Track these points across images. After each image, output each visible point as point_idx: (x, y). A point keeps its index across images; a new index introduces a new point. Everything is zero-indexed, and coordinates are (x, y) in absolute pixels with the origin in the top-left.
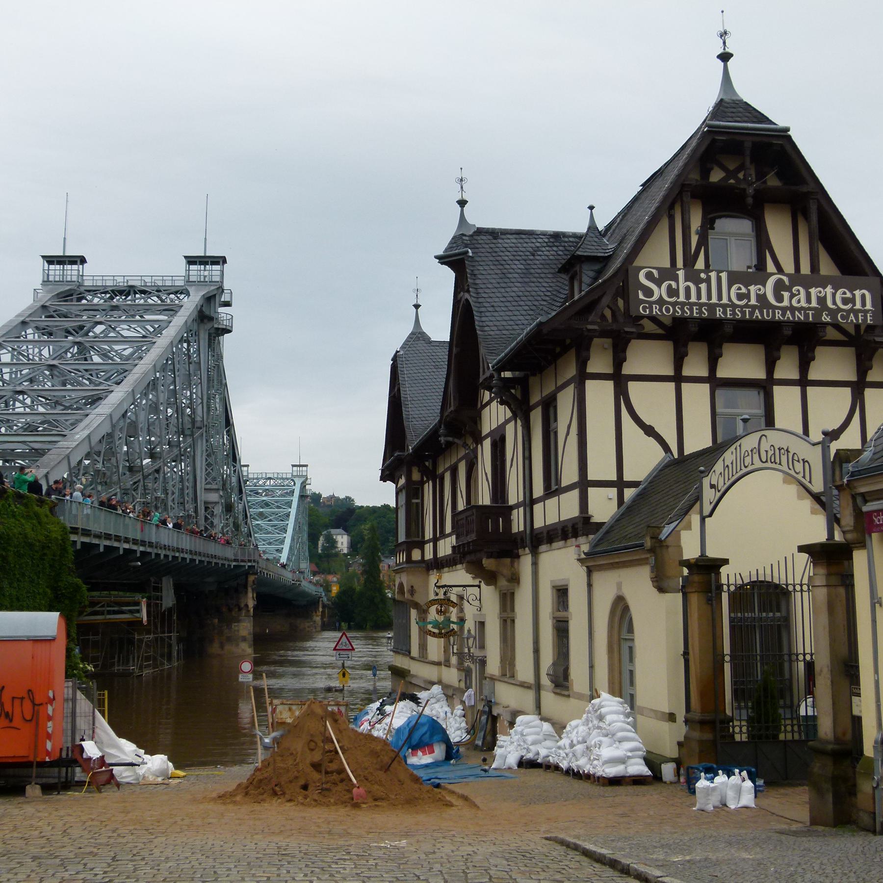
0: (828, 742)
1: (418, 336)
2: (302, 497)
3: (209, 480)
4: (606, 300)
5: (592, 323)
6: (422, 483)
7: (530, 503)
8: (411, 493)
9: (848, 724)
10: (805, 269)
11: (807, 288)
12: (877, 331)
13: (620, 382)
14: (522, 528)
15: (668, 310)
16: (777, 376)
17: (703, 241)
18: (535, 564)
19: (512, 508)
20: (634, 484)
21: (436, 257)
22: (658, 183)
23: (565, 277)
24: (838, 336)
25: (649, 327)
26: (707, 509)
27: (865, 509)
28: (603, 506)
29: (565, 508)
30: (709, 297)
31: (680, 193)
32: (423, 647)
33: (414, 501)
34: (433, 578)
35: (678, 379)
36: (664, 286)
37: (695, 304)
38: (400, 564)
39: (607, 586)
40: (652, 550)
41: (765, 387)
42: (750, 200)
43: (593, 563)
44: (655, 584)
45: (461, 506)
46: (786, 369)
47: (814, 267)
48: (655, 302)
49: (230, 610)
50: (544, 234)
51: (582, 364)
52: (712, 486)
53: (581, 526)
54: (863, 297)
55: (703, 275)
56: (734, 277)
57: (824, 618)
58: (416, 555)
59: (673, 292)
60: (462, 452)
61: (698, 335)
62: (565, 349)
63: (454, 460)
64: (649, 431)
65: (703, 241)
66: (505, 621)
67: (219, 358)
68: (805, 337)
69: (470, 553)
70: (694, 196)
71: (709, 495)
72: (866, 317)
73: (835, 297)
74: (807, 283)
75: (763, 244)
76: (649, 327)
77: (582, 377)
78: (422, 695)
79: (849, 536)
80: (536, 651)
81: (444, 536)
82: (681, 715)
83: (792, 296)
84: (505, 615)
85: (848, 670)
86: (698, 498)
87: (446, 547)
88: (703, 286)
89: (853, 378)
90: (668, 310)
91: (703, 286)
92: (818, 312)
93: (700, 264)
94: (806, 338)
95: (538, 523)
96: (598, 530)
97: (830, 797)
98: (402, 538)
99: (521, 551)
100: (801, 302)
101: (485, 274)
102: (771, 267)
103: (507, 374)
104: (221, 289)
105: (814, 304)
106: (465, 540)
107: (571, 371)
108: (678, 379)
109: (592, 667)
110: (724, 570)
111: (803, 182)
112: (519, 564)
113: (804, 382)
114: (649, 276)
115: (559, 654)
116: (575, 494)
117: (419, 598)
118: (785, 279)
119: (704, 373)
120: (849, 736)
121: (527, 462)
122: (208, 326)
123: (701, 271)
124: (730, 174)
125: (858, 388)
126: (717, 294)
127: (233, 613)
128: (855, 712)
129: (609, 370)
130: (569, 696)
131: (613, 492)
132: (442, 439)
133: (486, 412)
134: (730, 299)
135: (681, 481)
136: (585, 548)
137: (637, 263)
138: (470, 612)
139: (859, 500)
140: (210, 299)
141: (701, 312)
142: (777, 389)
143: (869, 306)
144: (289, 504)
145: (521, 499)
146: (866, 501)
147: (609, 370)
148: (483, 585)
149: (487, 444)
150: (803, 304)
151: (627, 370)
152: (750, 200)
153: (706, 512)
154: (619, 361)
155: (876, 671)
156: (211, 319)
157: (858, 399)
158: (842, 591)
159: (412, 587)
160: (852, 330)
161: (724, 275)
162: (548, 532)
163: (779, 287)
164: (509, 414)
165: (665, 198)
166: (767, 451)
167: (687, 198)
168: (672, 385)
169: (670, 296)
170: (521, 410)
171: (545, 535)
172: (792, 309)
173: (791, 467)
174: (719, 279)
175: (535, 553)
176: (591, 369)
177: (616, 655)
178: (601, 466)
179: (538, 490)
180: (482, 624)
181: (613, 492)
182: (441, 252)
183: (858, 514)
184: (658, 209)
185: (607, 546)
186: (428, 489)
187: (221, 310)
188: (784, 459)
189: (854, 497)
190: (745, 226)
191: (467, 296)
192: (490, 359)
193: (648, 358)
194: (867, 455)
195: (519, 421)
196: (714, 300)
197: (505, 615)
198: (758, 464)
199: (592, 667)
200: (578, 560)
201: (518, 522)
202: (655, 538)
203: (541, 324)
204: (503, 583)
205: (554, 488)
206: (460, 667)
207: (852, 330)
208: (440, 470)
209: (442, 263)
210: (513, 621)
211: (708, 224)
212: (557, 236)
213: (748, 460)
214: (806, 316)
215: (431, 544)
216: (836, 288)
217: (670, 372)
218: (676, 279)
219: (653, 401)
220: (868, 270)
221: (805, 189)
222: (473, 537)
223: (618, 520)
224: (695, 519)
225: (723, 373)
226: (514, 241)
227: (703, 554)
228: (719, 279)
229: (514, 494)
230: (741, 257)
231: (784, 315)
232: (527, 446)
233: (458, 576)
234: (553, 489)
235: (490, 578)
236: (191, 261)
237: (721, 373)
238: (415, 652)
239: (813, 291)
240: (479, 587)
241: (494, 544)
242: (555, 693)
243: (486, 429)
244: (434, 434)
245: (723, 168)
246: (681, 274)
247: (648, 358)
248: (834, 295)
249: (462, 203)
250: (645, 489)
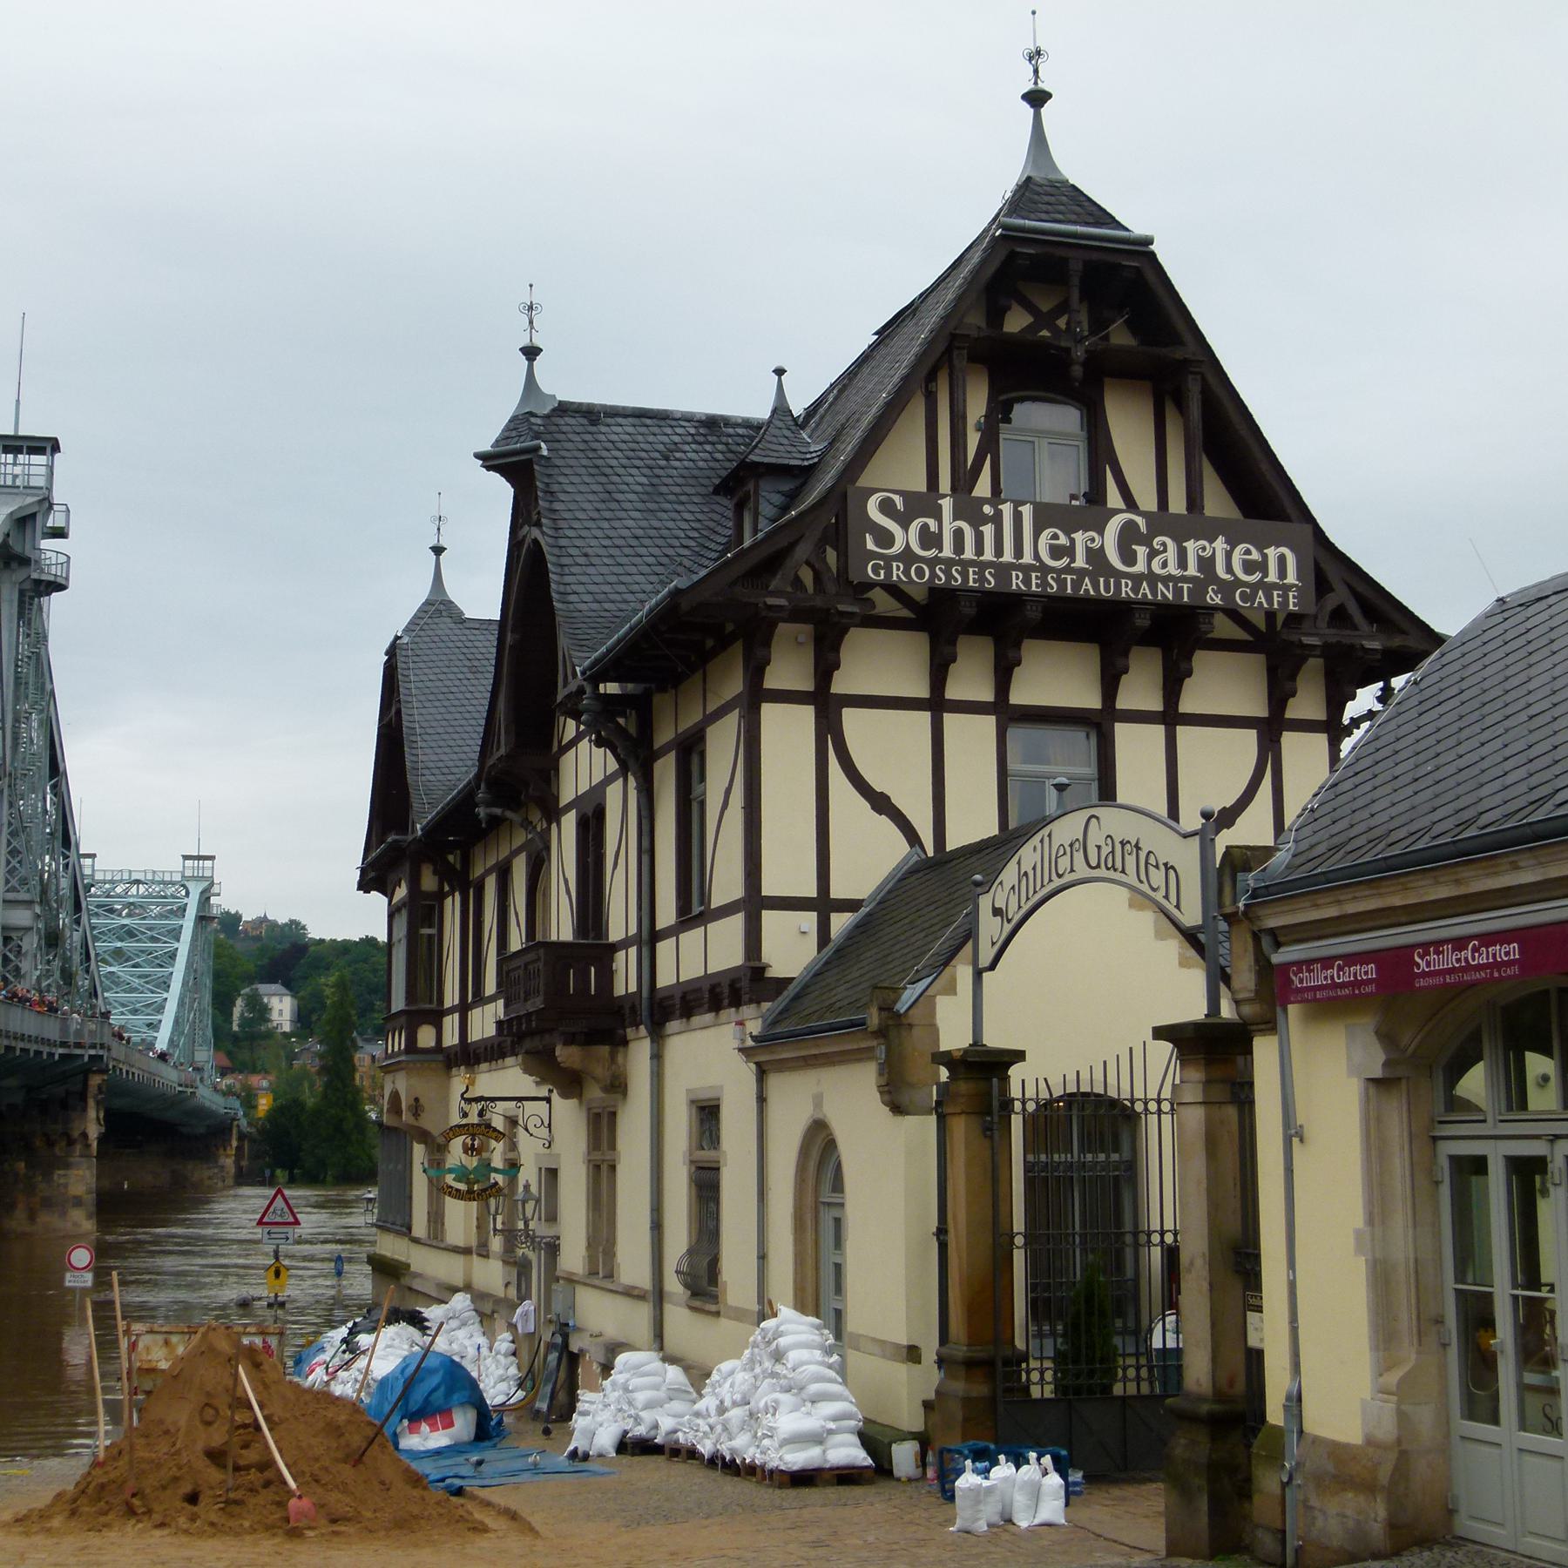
0: (1201, 1399)
1: (438, 607)
2: (203, 919)
3: (14, 882)
4: (803, 551)
5: (777, 593)
6: (440, 896)
7: (650, 937)
8: (418, 915)
9: (1238, 1363)
10: (1177, 504)
11: (1179, 541)
12: (1306, 625)
13: (828, 710)
14: (633, 988)
15: (920, 573)
16: (1122, 704)
17: (990, 444)
18: (657, 1057)
19: (614, 948)
20: (850, 905)
21: (477, 456)
22: (909, 328)
23: (726, 504)
24: (1240, 634)
25: (884, 604)
26: (985, 958)
27: (1276, 958)
28: (790, 947)
29: (716, 949)
30: (999, 551)
31: (948, 351)
32: (436, 1218)
33: (425, 931)
34: (458, 1082)
35: (937, 705)
36: (915, 526)
37: (972, 563)
38: (393, 1055)
39: (796, 1099)
40: (881, 1033)
41: (1099, 725)
42: (1077, 371)
44: (887, 1097)
45: (516, 942)
46: (1139, 691)
47: (1194, 501)
48: (897, 558)
49: (51, 1144)
50: (688, 418)
51: (756, 672)
52: (997, 912)
53: (747, 984)
54: (1282, 560)
55: (987, 509)
56: (1046, 516)
57: (1198, 1166)
58: (426, 1037)
59: (930, 539)
60: (520, 838)
61: (976, 621)
62: (724, 643)
63: (504, 853)
64: (881, 803)
65: (990, 444)
66: (597, 1167)
67: (41, 639)
68: (1173, 633)
69: (532, 1034)
70: (973, 359)
71: (990, 929)
72: (1285, 597)
73: (1230, 558)
74: (1181, 531)
75: (1100, 455)
76: (884, 604)
77: (755, 697)
78: (433, 1313)
79: (1247, 1010)
80: (657, 1227)
81: (480, 1000)
82: (930, 1347)
83: (1153, 554)
84: (597, 1156)
85: (1240, 1262)
86: (970, 934)
87: (484, 1023)
88: (988, 530)
89: (1260, 710)
90: (920, 573)
91: (988, 530)
92: (1199, 586)
93: (983, 488)
94: (1173, 633)
95: (665, 978)
96: (779, 993)
97: (1203, 1504)
98: (398, 1003)
99: (630, 1032)
100: (1169, 566)
101: (573, 493)
102: (1114, 499)
103: (612, 688)
104: (47, 503)
105: (1192, 570)
106: (522, 1009)
107: (734, 686)
109: (762, 1257)
110: (1016, 1072)
111: (1174, 339)
112: (626, 1056)
113: (1171, 718)
114: (887, 507)
115: (700, 1231)
116: (737, 922)
117: (429, 1122)
118: (1140, 521)
119: (986, 695)
120: (1240, 1387)
121: (645, 859)
122: (20, 575)
123: (983, 501)
124: (1041, 319)
125: (1270, 730)
126: (1015, 546)
127: (57, 1150)
128: (1253, 1342)
129: (807, 685)
130: (717, 1314)
131: (809, 919)
132: (482, 812)
133: (568, 760)
134: (1037, 556)
135: (937, 903)
136: (755, 1027)
137: (864, 481)
138: (530, 1150)
139: (1266, 942)
141: (981, 579)
142: (1122, 731)
143: (1291, 578)
144: (176, 934)
145: (633, 930)
146: (1278, 945)
147: (807, 685)
148: (555, 1097)
149: (569, 822)
150: (1172, 569)
151: (841, 684)
152: (1077, 371)
153: (984, 961)
154: (825, 668)
155: (1291, 1264)
156: (25, 562)
157: (1269, 750)
158: (1231, 1112)
159: (417, 1100)
160: (1262, 626)
161: (1027, 511)
162: (683, 998)
163: (1129, 536)
164: (613, 765)
165: (920, 359)
166: (1099, 847)
167: (960, 360)
168: (925, 717)
169: (924, 547)
170: (636, 758)
171: (677, 1001)
172: (1152, 578)
173: (1143, 877)
174: (1018, 517)
175: (658, 1036)
176: (775, 679)
177: (810, 1235)
178: (788, 871)
179: (666, 915)
180: (552, 1174)
181: (809, 919)
182: (486, 446)
183: (1265, 969)
184: (906, 379)
185: (801, 1024)
186: (452, 908)
187: (46, 544)
188: (1131, 861)
189: (1256, 937)
190: (1066, 418)
191: (535, 533)
192: (578, 657)
193: (880, 664)
194: (1281, 858)
195: (631, 779)
196: (1008, 557)
197: (597, 1156)
198: (1082, 871)
199: (762, 1257)
200: (740, 1050)
201: (626, 976)
202: (887, 1009)
203: (677, 592)
204: (594, 1092)
205: (696, 909)
206: (509, 1257)
207: (1262, 626)
208: (478, 871)
209: (489, 468)
210: (613, 1168)
211: (999, 412)
212: (713, 424)
213: (1064, 863)
214: (1178, 592)
215: (456, 1016)
216: (1232, 543)
217: (923, 692)
218: (938, 517)
219: (888, 746)
220: (1291, 511)
221: (1178, 354)
222: (536, 1004)
223: (818, 975)
224: (963, 973)
225: (1022, 694)
226: (631, 430)
227: (977, 1041)
228: (1018, 517)
229: (620, 921)
230: (1059, 478)
231: (1136, 589)
232: (645, 828)
233: (508, 1080)
235: (571, 1083)
237: (1017, 697)
238: (420, 1227)
239: (1191, 546)
240: (548, 1100)
241: (578, 1017)
242: (692, 1308)
243: (567, 795)
244: (466, 801)
245: (1030, 307)
246: (947, 504)
247: (880, 664)
248: (1229, 555)
249: (531, 352)
250: (869, 914)
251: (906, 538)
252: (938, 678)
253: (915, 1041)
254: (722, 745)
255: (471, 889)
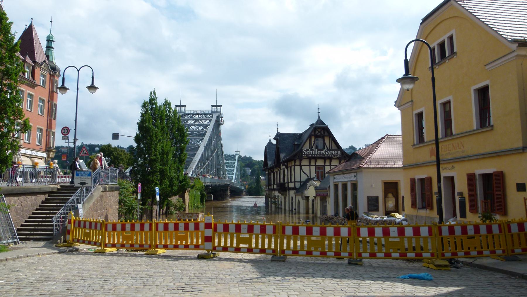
7: (288, 183)
13: (301, 166)
28: (298, 185)
34: (273, 192)
35: (310, 165)
43: (296, 194)
46: (327, 163)
51: (295, 163)
53: (294, 188)
58: (270, 187)
59: (308, 153)
68: (330, 158)
73: (334, 153)
74: (330, 150)
75: (324, 143)
77: (295, 165)
93: (314, 148)
94: (330, 158)
100: (329, 153)
104: (221, 114)
108: (310, 165)
116: (293, 184)
126: (316, 153)
140: (218, 117)
144: (235, 163)
151: (302, 164)
154: (300, 163)
163: (325, 151)
178: (298, 179)
186: (272, 174)
219: (306, 169)
229: (286, 181)
233: (276, 193)
234: (291, 182)
235: (282, 194)
236: (213, 106)
247: (305, 162)
251: (306, 153)
252: (310, 163)
253: (304, 195)
254: (293, 168)
255: (274, 173)
